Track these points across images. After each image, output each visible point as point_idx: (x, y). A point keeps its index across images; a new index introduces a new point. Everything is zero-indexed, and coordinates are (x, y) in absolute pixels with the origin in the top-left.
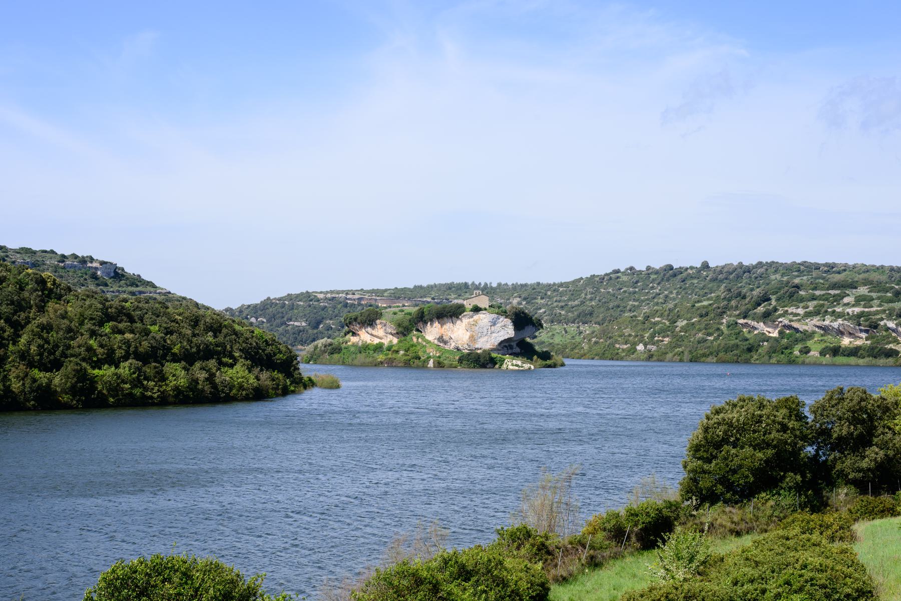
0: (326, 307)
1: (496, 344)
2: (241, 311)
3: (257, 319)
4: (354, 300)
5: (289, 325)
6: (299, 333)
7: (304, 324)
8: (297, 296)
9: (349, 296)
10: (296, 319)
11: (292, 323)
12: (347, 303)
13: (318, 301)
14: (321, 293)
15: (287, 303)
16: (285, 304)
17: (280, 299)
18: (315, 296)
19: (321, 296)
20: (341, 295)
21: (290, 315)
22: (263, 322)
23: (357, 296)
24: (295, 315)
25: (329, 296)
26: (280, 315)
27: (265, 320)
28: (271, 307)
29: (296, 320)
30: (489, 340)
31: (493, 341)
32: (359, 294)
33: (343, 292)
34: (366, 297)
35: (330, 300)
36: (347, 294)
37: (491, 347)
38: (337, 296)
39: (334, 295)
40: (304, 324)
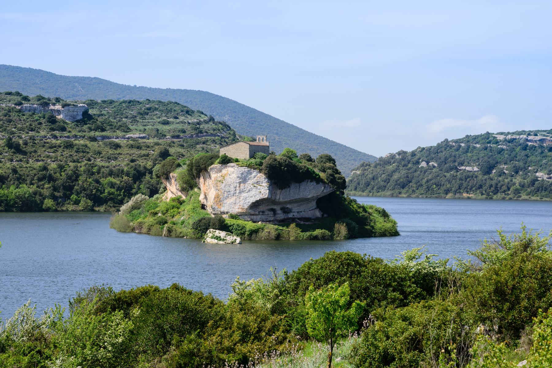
0: (503, 150)
1: (246, 207)
2: (413, 154)
3: (428, 163)
4: (536, 141)
5: (460, 170)
6: (466, 179)
7: (476, 169)
8: (476, 137)
9: (530, 138)
10: (468, 163)
11: (463, 168)
12: (527, 145)
13: (497, 142)
14: (502, 134)
15: (463, 145)
16: (460, 146)
17: (456, 141)
18: (495, 138)
19: (501, 138)
20: (521, 136)
21: (463, 158)
22: (434, 167)
23: (538, 138)
24: (467, 159)
25: (509, 137)
26: (452, 158)
27: (436, 165)
28: (445, 150)
29: (469, 165)
30: (238, 201)
31: (241, 203)
32: (541, 135)
33: (523, 132)
34: (548, 138)
35: (509, 142)
36: (529, 135)
37: (240, 210)
38: (518, 137)
39: (514, 137)
40: (476, 169)
